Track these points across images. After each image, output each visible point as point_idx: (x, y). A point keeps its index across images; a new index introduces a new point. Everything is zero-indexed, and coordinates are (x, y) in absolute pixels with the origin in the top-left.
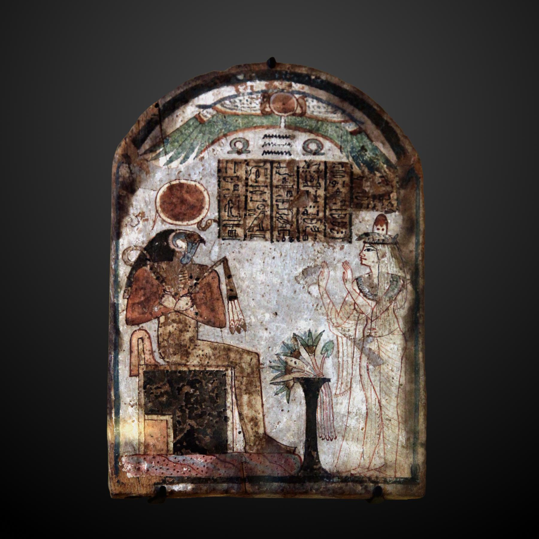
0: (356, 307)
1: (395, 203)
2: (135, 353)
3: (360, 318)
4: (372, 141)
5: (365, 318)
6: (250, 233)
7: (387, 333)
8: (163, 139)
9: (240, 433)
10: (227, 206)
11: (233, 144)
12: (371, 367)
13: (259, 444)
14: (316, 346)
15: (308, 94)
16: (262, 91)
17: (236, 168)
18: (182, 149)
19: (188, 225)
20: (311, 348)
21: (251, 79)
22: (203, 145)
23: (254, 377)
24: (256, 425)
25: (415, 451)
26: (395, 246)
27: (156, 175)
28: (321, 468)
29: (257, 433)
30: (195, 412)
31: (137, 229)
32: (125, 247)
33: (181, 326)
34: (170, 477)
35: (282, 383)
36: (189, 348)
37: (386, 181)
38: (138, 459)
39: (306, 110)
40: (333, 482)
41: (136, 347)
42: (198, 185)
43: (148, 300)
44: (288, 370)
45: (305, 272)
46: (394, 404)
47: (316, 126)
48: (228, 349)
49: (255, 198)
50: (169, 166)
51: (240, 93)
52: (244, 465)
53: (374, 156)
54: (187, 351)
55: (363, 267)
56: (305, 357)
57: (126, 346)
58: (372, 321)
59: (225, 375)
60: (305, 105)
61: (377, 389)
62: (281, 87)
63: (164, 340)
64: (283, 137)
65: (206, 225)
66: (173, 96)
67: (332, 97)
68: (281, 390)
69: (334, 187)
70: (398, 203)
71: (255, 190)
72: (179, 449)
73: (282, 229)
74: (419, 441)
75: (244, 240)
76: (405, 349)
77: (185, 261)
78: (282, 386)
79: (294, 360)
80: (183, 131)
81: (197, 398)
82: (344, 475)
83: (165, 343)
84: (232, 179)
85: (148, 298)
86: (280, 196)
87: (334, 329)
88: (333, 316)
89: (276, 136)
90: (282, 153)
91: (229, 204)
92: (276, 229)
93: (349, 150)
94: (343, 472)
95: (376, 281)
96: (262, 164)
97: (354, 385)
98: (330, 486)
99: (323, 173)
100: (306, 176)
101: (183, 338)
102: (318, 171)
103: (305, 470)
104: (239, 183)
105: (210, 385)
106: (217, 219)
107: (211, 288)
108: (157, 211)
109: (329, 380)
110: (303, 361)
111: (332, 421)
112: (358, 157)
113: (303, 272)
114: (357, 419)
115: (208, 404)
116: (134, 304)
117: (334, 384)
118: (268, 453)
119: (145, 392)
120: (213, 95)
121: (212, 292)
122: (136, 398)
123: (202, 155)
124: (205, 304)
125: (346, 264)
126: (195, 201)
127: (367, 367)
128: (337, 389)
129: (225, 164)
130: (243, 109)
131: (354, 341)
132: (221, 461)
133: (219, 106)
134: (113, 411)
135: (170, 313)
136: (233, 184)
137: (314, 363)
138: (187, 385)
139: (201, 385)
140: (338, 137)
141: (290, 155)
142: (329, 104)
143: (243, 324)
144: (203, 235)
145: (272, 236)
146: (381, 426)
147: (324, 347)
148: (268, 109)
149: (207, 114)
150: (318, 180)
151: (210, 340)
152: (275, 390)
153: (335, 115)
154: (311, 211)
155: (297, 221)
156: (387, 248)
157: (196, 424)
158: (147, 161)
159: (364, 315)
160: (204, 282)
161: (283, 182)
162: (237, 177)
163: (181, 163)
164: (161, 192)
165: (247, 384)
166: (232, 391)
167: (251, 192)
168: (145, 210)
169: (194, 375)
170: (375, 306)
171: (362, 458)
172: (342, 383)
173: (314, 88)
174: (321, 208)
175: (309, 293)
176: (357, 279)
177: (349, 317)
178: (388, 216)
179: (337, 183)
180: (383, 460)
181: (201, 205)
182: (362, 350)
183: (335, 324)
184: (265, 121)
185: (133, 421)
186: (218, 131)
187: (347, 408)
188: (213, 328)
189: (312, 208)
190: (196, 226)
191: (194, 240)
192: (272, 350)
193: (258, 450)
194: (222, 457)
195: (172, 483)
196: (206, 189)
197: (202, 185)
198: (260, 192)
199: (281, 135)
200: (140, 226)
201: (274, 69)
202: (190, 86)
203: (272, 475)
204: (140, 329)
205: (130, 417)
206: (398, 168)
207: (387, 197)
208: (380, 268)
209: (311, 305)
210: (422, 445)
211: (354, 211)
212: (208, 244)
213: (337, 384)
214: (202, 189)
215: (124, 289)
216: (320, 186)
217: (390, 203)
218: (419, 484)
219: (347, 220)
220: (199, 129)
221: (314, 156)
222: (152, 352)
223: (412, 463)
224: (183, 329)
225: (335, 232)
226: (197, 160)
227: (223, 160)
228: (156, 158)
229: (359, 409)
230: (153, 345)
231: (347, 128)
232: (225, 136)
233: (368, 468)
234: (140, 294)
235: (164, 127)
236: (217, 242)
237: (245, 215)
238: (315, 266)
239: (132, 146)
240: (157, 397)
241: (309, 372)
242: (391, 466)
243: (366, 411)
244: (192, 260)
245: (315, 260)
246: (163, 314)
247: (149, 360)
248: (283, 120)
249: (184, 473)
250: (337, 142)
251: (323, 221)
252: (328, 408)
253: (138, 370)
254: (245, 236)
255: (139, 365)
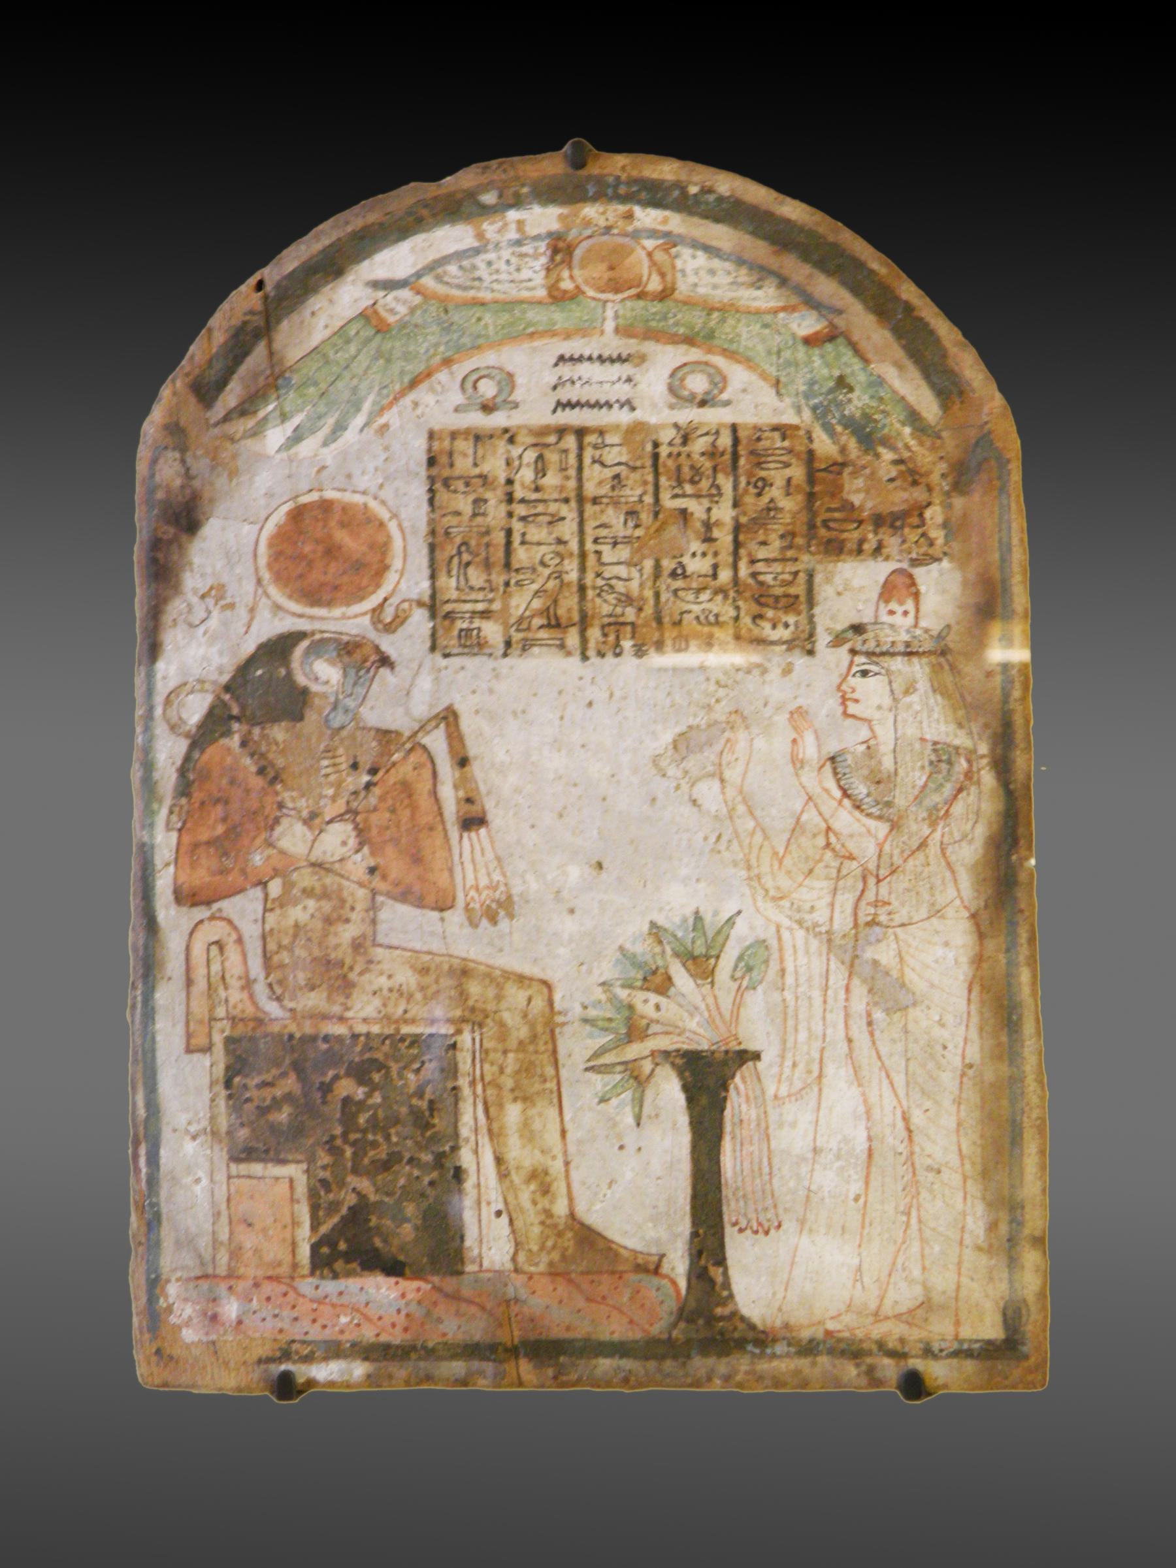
0: (833, 839)
1: (938, 535)
2: (201, 985)
3: (844, 872)
4: (866, 361)
5: (859, 872)
6: (521, 635)
7: (923, 913)
8: (277, 379)
9: (499, 1214)
10: (456, 561)
11: (469, 385)
12: (878, 1015)
13: (554, 1247)
14: (718, 957)
15: (679, 236)
16: (550, 234)
17: (480, 452)
18: (327, 405)
19: (344, 617)
20: (701, 964)
21: (518, 202)
22: (385, 391)
23: (536, 1052)
24: (546, 1190)
25: (1013, 1262)
26: (942, 660)
27: (257, 478)
28: (735, 1314)
29: (548, 1213)
30: (371, 1153)
31: (205, 633)
32: (172, 684)
33: (327, 906)
34: (303, 1342)
35: (619, 1068)
36: (351, 968)
37: (912, 475)
38: (210, 1290)
39: (674, 283)
40: (774, 1356)
41: (210, 964)
42: (373, 505)
43: (233, 833)
44: (634, 1030)
45: (683, 744)
46: (949, 1122)
47: (705, 323)
48: (464, 972)
49: (536, 533)
50: (293, 451)
51: (488, 242)
52: (515, 1309)
53: (874, 404)
54: (345, 977)
55: (849, 721)
56: (683, 990)
57: (174, 964)
58: (879, 881)
59: (454, 1046)
60: (674, 267)
61: (899, 1080)
62: (602, 223)
63: (280, 946)
64: (612, 361)
65: (396, 616)
66: (304, 258)
67: (748, 240)
68: (616, 1090)
69: (759, 495)
70: (946, 536)
71: (533, 511)
72: (326, 1259)
73: (612, 620)
74: (1027, 1231)
75: (505, 655)
76: (978, 960)
77: (338, 719)
78: (618, 1077)
79: (654, 998)
80: (331, 354)
81: (375, 1116)
82: (806, 1334)
83: (285, 957)
84: (467, 484)
85: (234, 827)
86: (603, 526)
87: (769, 905)
88: (765, 868)
89: (590, 358)
90: (609, 405)
91: (459, 553)
92: (597, 622)
93: (803, 388)
94: (801, 1327)
95: (888, 763)
96: (552, 439)
97: (830, 1069)
98: (763, 1366)
99: (727, 457)
100: (679, 468)
101: (332, 941)
102: (712, 453)
103: (690, 1321)
104: (488, 495)
105: (411, 1076)
106: (426, 598)
107: (410, 796)
108: (259, 582)
109: (757, 1056)
110: (680, 999)
111: (767, 1178)
112: (827, 410)
113: (675, 745)
114: (842, 1168)
115: (408, 1130)
116: (196, 846)
117: (771, 1066)
118: (582, 1273)
119: (230, 1097)
120: (413, 250)
121: (414, 808)
122: (204, 1114)
123: (382, 421)
124: (396, 841)
125: (799, 716)
126: (364, 548)
127: (869, 1015)
128: (779, 1081)
129: (447, 443)
130: (495, 286)
131: (829, 939)
132: (447, 1296)
133: (428, 281)
134: (142, 1151)
135: (296, 869)
136: (471, 498)
137: (713, 1007)
138: (348, 1074)
139: (387, 1075)
140: (769, 353)
141: (633, 409)
142: (740, 262)
143: (503, 897)
144: (387, 644)
145: (584, 641)
146: (913, 1187)
147: (740, 958)
148: (567, 285)
149: (397, 305)
150: (715, 478)
151: (411, 945)
152: (599, 1087)
153: (759, 293)
154: (697, 566)
155: (657, 595)
156: (918, 667)
157: (372, 1189)
158: (232, 440)
159: (854, 864)
160: (393, 778)
161: (613, 488)
162: (483, 477)
163: (325, 444)
164: (270, 528)
165: (517, 1072)
166: (474, 1093)
167: (523, 519)
168: (225, 579)
169: (368, 1048)
170: (886, 837)
171: (858, 1284)
172: (794, 1065)
173: (696, 220)
174: (726, 557)
175: (694, 802)
176: (832, 759)
177: (811, 871)
178: (919, 573)
179: (766, 483)
180: (918, 1290)
181: (382, 561)
182: (852, 965)
183: (772, 893)
184: (559, 317)
185: (198, 1181)
186: (427, 351)
187: (810, 1137)
188: (418, 912)
189: (698, 558)
190: (366, 620)
191: (363, 659)
192: (590, 972)
193: (551, 1264)
194: (450, 1284)
195: (308, 1359)
196: (395, 516)
197: (383, 503)
198: (548, 519)
199: (606, 354)
200: (214, 623)
201: (583, 173)
202: (349, 229)
203: (594, 1337)
204: (212, 918)
205: (189, 1170)
206: (944, 434)
207: (915, 520)
208: (900, 726)
209: (701, 835)
210: (1037, 1241)
211: (820, 562)
212: (403, 671)
213: (781, 1065)
214: (384, 514)
215: (168, 802)
216: (720, 494)
217: (924, 535)
218: (1027, 1357)
219: (799, 589)
220: (374, 344)
221: (701, 410)
222: (248, 984)
223: (1006, 1294)
224: (335, 915)
225: (767, 626)
226: (370, 433)
227: (441, 431)
228: (256, 432)
229: (846, 1140)
230: (250, 963)
231: (794, 326)
232: (447, 362)
233: (876, 1314)
234: (213, 816)
235: (277, 346)
236: (428, 663)
237: (507, 584)
238: (709, 726)
239: (192, 400)
240: (263, 1111)
241: (699, 1034)
242: (943, 1307)
243: (866, 1146)
244: (356, 718)
245: (709, 708)
246: (276, 873)
247: (240, 1006)
248: (610, 313)
249: (342, 1332)
250: (766, 367)
251: (732, 594)
252: (756, 1138)
253: (210, 1035)
254: (508, 644)
255: (213, 1019)
